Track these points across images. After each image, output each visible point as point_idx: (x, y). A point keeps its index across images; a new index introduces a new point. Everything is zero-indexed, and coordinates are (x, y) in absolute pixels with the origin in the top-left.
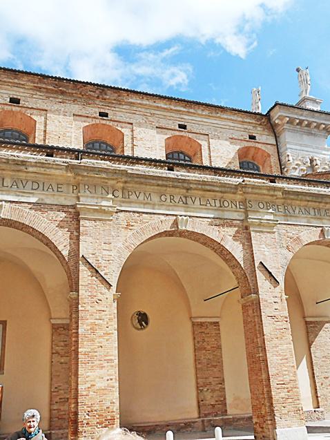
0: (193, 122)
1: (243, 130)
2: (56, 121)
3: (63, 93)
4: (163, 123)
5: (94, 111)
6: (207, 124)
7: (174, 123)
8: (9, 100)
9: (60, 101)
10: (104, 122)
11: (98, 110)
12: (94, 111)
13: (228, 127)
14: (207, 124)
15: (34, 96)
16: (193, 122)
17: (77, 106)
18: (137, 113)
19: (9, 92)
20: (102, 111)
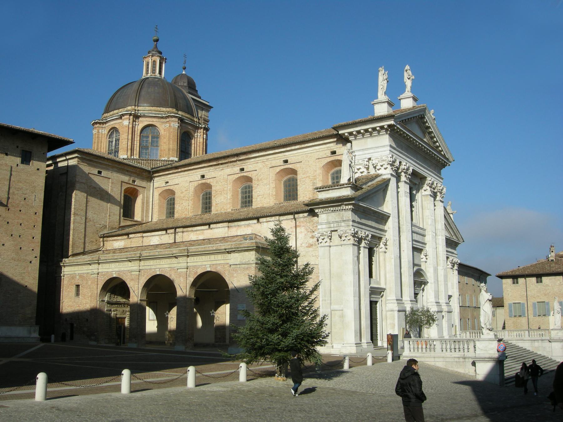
0: (292, 155)
1: (326, 149)
2: (220, 183)
3: (222, 164)
4: (274, 163)
5: (237, 169)
6: (301, 154)
7: (280, 161)
8: (200, 177)
9: (221, 169)
10: (242, 174)
11: (239, 168)
12: (237, 169)
13: (315, 151)
14: (301, 154)
15: (210, 171)
16: (292, 155)
17: (229, 169)
18: (259, 162)
19: (200, 173)
20: (241, 167)
